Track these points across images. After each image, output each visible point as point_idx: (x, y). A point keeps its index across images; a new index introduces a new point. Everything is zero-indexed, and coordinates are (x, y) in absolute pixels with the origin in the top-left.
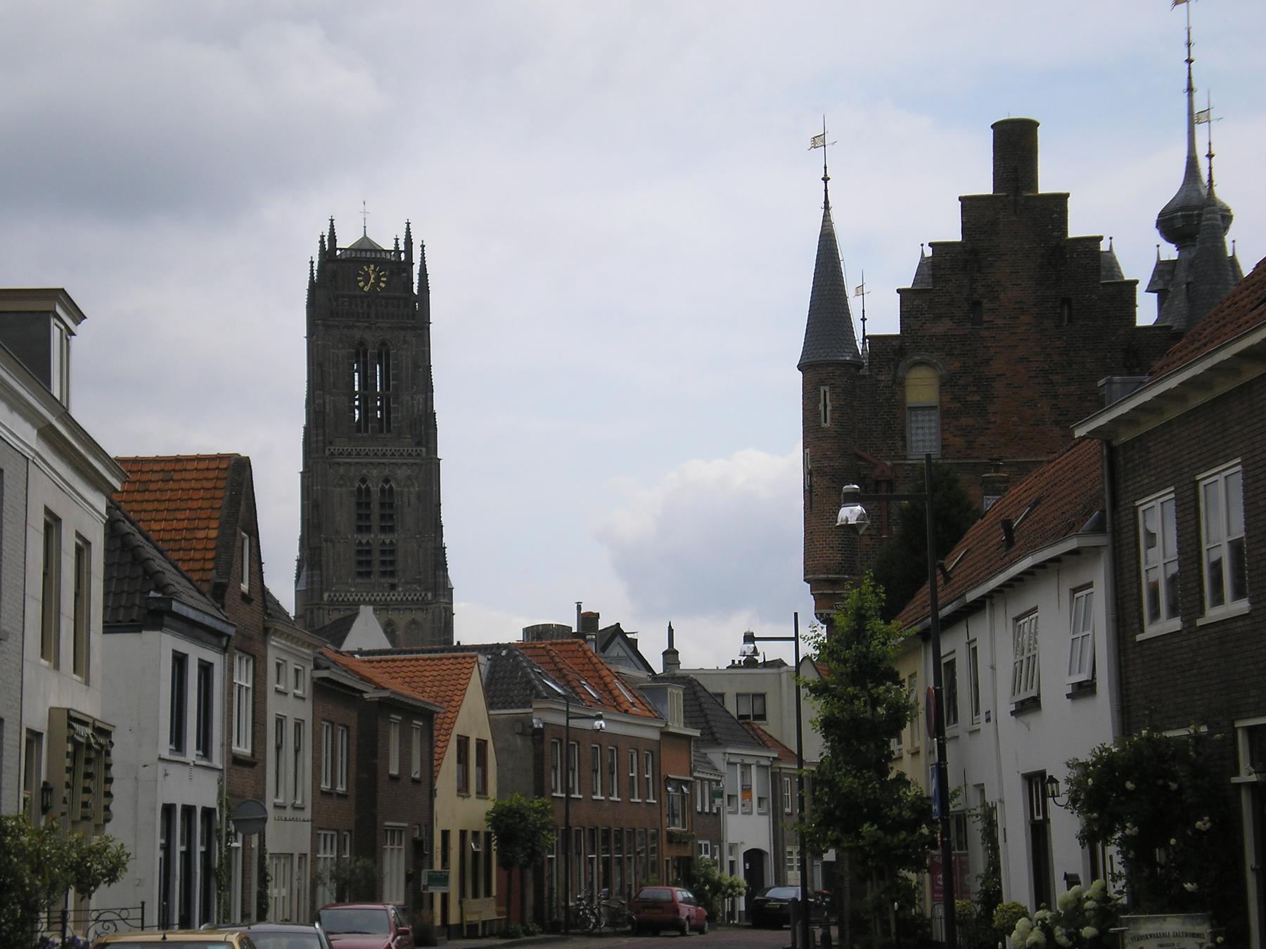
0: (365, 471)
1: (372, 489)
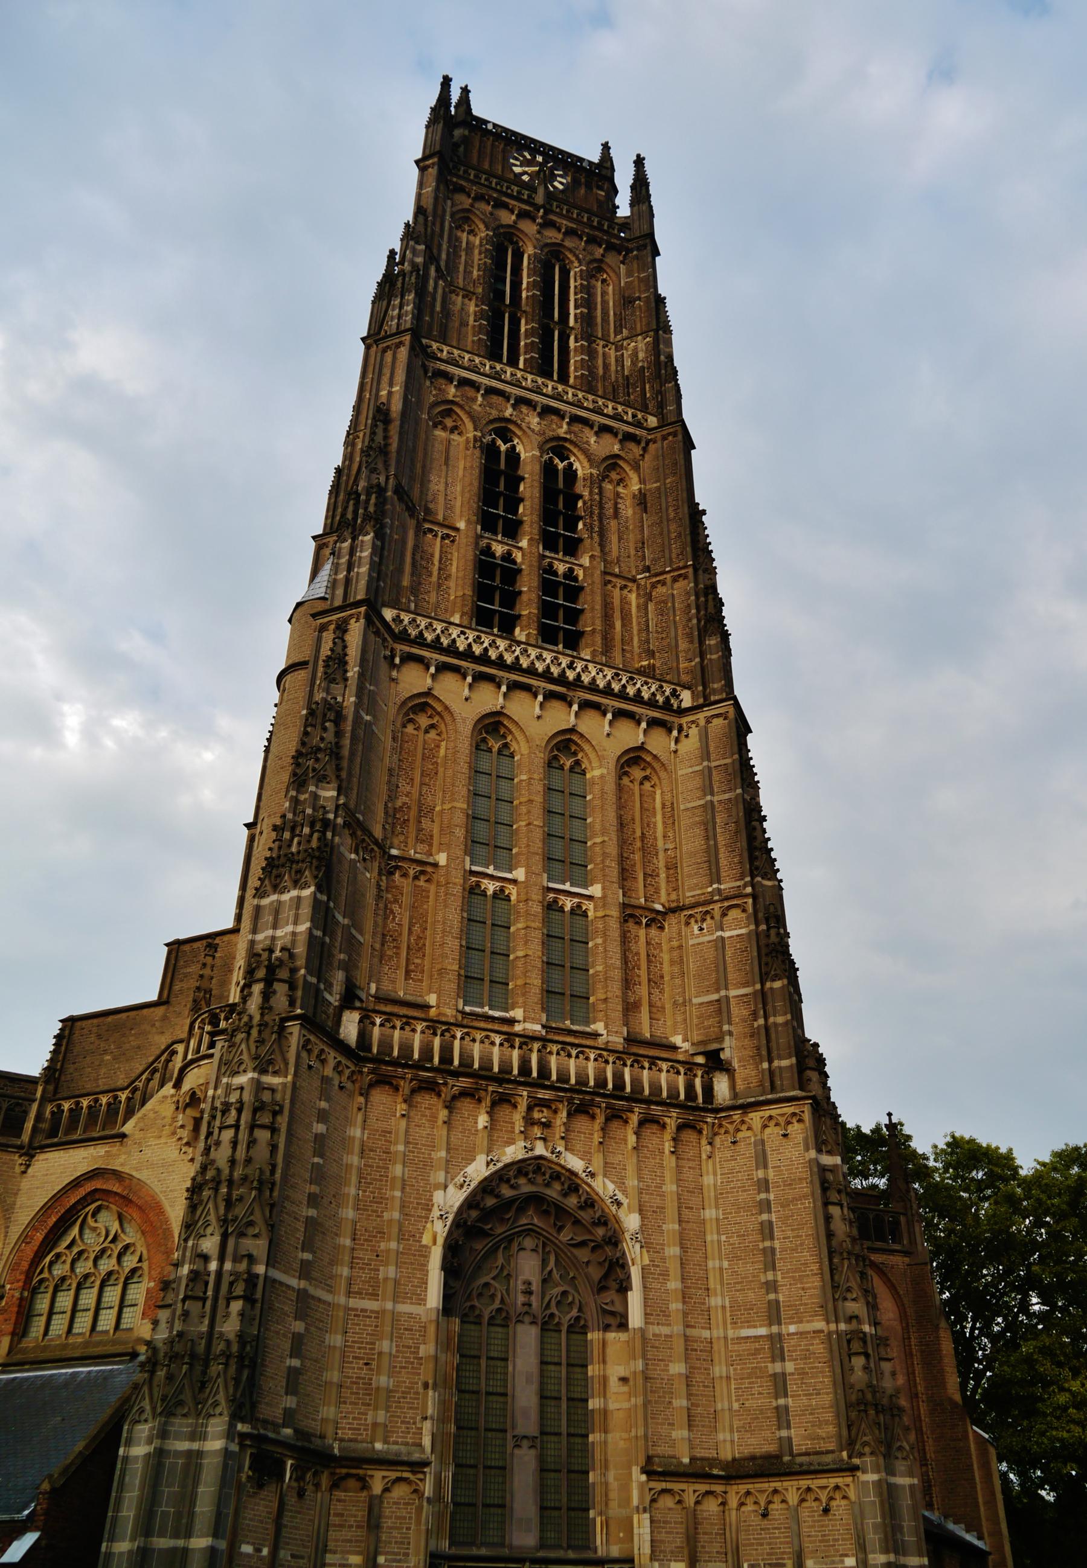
0: (509, 412)
1: (523, 456)
